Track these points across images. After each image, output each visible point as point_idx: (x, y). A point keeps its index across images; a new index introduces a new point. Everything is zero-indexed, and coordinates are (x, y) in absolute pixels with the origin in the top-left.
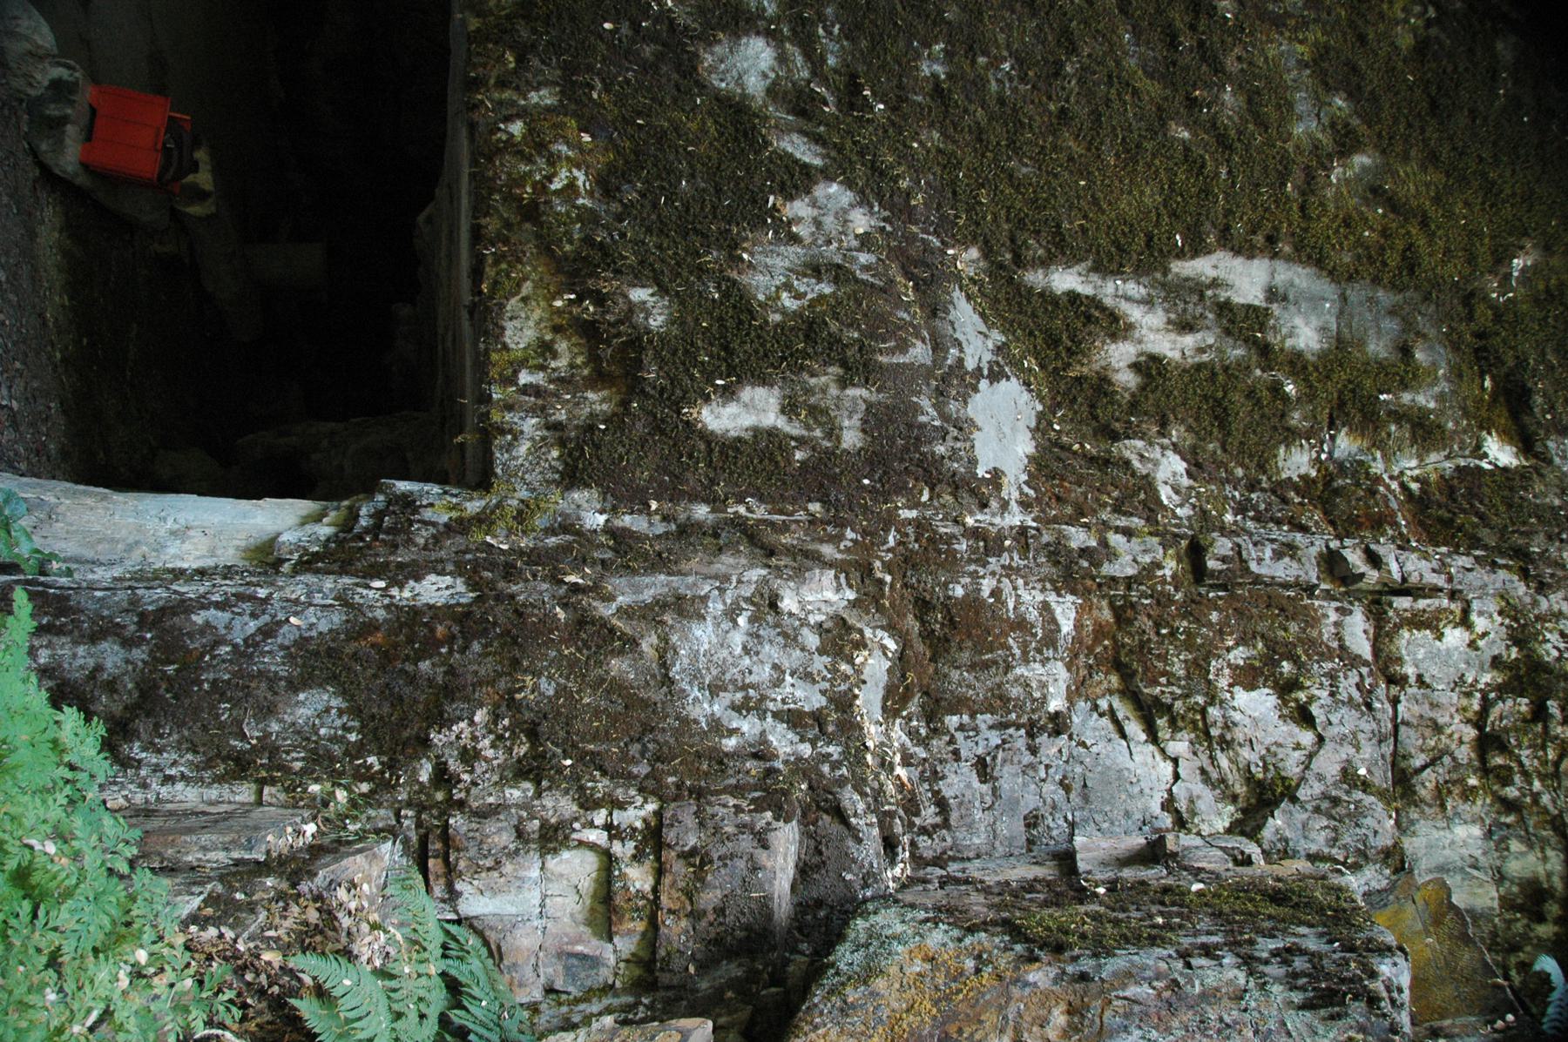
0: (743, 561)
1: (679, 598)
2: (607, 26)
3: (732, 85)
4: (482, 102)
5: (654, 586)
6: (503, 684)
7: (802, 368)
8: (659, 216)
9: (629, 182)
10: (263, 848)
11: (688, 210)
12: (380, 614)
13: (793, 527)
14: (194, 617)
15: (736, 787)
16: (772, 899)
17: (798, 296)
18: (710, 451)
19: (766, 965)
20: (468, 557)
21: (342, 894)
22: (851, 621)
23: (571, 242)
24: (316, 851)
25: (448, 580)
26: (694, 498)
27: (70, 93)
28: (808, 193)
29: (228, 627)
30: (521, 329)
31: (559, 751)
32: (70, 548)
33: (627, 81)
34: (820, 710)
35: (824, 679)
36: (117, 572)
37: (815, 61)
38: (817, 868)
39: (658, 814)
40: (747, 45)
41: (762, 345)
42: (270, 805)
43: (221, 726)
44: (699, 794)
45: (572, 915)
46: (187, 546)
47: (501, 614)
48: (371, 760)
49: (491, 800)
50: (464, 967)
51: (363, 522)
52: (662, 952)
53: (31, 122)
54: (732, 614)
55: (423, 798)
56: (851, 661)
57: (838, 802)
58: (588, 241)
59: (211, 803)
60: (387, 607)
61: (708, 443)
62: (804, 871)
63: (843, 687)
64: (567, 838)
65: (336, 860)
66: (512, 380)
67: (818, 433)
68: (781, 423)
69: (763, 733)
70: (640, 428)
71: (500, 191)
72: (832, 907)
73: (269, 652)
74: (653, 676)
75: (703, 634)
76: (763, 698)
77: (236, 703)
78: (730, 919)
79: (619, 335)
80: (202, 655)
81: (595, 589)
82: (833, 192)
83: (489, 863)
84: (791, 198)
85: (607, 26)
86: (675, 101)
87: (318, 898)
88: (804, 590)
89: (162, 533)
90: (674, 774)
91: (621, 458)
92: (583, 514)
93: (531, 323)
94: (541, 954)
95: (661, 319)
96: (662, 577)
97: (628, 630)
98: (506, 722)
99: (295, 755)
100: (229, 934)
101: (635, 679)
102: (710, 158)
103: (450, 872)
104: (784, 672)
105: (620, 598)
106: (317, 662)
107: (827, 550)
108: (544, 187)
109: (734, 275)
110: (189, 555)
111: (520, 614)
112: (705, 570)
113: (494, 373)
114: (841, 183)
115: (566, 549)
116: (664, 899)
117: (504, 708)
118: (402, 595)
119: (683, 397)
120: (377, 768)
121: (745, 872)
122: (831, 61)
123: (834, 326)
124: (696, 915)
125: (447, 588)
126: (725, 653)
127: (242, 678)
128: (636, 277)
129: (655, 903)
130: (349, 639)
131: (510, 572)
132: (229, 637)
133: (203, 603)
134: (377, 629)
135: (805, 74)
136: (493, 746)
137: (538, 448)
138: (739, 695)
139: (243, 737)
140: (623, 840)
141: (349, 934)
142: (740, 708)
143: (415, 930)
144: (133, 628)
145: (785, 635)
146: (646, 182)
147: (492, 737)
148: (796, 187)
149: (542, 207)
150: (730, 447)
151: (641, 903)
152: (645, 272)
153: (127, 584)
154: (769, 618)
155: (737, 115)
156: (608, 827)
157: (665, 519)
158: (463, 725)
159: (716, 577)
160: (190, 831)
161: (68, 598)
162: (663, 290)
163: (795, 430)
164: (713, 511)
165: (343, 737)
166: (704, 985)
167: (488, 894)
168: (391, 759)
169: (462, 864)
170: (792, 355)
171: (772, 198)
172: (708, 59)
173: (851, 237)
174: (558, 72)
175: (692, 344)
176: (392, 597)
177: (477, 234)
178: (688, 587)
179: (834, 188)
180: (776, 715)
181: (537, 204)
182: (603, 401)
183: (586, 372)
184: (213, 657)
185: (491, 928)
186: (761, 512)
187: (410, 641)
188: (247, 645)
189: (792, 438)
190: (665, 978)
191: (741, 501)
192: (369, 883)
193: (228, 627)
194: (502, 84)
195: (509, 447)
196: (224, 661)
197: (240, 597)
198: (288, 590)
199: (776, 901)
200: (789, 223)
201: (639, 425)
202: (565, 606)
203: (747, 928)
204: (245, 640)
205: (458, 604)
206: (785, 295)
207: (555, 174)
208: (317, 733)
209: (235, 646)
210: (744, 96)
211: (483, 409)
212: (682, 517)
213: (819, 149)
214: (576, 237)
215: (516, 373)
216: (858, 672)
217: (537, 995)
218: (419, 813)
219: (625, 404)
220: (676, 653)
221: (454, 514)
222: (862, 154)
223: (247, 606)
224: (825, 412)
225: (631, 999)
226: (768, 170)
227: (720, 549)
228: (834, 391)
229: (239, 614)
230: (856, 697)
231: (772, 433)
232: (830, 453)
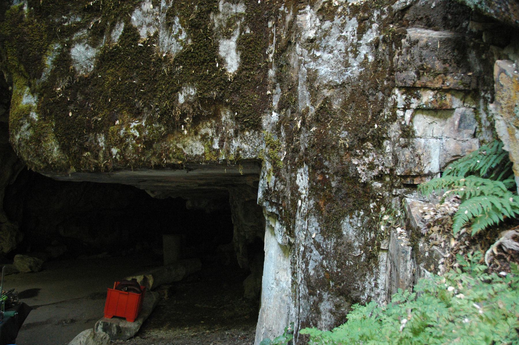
0: (293, 54)
1: (308, 80)
2: (70, 114)
3: (92, 63)
4: (104, 165)
5: (303, 91)
6: (342, 153)
7: (211, 30)
8: (149, 92)
9: (135, 104)
10: (407, 247)
11: (146, 80)
12: (312, 202)
13: (278, 33)
14: (311, 274)
15: (390, 55)
16: (441, 38)
17: (180, 32)
18: (246, 69)
19: (472, 41)
20: (289, 167)
21: (427, 217)
22: (320, 7)
23: (160, 128)
24: (408, 227)
25: (298, 175)
26: (266, 76)
28: (136, 29)
29: (316, 261)
30: (196, 148)
31: (371, 129)
32: (283, 323)
33: (93, 106)
34: (358, 20)
35: (344, 19)
36: (292, 306)
37: (79, 27)
38: (428, 19)
39: (400, 88)
40: (74, 56)
41: (201, 47)
42: (388, 246)
43: (356, 264)
44: (392, 71)
45: (442, 126)
46: (283, 279)
47: (312, 153)
48: (371, 206)
49: (390, 158)
50: (461, 170)
51: (274, 210)
52: (461, 87)
54: (315, 58)
55: (388, 185)
56: (337, 7)
57: (399, 10)
58: (160, 121)
59: (387, 269)
60: (309, 199)
61: (243, 70)
62: (429, 25)
63: (348, 10)
64: (408, 127)
65: (413, 219)
66: (217, 151)
67: (238, 23)
68: (234, 39)
69: (367, 44)
70: (237, 98)
71: (141, 157)
72: (447, 12)
73: (326, 245)
74: (341, 91)
75: (323, 70)
76: (352, 44)
77: (347, 259)
78: (449, 57)
79: (198, 107)
80: (327, 271)
81: (303, 115)
82: (136, 18)
83: (417, 159)
84: (139, 36)
85: (70, 114)
86: (100, 86)
87: (429, 226)
88: (305, 28)
89: (277, 289)
90: (383, 82)
91: (249, 106)
92: (272, 121)
93: (194, 144)
94: (458, 139)
95: (191, 90)
96: (299, 88)
97: (321, 101)
98: (358, 151)
100: (442, 260)
101: (342, 98)
102: (123, 71)
103: (421, 175)
104: (341, 36)
105: (308, 105)
106: (331, 226)
107: (288, 18)
109: (172, 60)
110: (286, 278)
111: (313, 146)
112: (297, 70)
113: (214, 159)
114: (131, 15)
115: (286, 128)
116: (438, 86)
117: (352, 152)
118: (304, 193)
119: (224, 80)
120: (375, 204)
121: (428, 50)
122: (79, 20)
123: (193, 16)
124: (446, 72)
125: (302, 176)
126: (332, 61)
127: (336, 256)
128: (174, 100)
129: (439, 90)
130: (322, 214)
131: (296, 150)
132: (320, 261)
133: (306, 271)
134: (318, 203)
135: (85, 31)
136: (368, 157)
137: (245, 140)
138: (350, 55)
139: (360, 256)
140: (410, 103)
141: (444, 215)
142: (356, 55)
143: (445, 186)
144: (315, 298)
145: (325, 36)
146: (134, 97)
147: (364, 157)
148: (134, 34)
149: (147, 140)
150: (244, 60)
151: (438, 96)
152: (172, 97)
153: (297, 301)
154: (317, 42)
155: (104, 60)
156: (404, 110)
157: (274, 88)
158: (358, 169)
159: (299, 66)
160: (398, 276)
161: (303, 322)
162: (179, 89)
163: (237, 33)
164: (271, 68)
165: (362, 217)
166: (478, 68)
167: (430, 160)
168: (372, 198)
169: (417, 170)
170: (206, 35)
171: (139, 45)
172: (82, 73)
173: (154, 10)
174: (91, 134)
175: (202, 77)
176: (305, 198)
177: (158, 167)
178: (303, 77)
179: (134, 18)
180: (359, 39)
181: (145, 142)
182: (225, 114)
183: (214, 121)
184: (328, 267)
185: (445, 159)
186: (272, 48)
187: (323, 190)
188: (323, 254)
189: (241, 34)
190: (473, 85)
191: (267, 56)
192: (423, 207)
193: (316, 261)
194: (97, 157)
195: (245, 152)
196: (329, 263)
197: (304, 257)
198: (301, 239)
199: (442, 36)
200: (149, 37)
201: (236, 99)
202: (310, 127)
203: (453, 50)
204: (321, 255)
205: (308, 171)
206: (180, 38)
207: (133, 135)
208: (360, 227)
209: (323, 259)
210: (96, 57)
211: (229, 163)
212: (274, 81)
213: (117, 25)
214: (158, 126)
215: (214, 150)
216: (342, 4)
217: (476, 141)
218: (395, 187)
219: (227, 105)
220: (331, 81)
221: (272, 174)
222: (118, 6)
223: (307, 254)
224: (229, 20)
225: (482, 101)
226: (127, 46)
227: (288, 64)
228: (220, 16)
229: (310, 257)
230: (353, 5)
231: (238, 43)
232: (247, 18)
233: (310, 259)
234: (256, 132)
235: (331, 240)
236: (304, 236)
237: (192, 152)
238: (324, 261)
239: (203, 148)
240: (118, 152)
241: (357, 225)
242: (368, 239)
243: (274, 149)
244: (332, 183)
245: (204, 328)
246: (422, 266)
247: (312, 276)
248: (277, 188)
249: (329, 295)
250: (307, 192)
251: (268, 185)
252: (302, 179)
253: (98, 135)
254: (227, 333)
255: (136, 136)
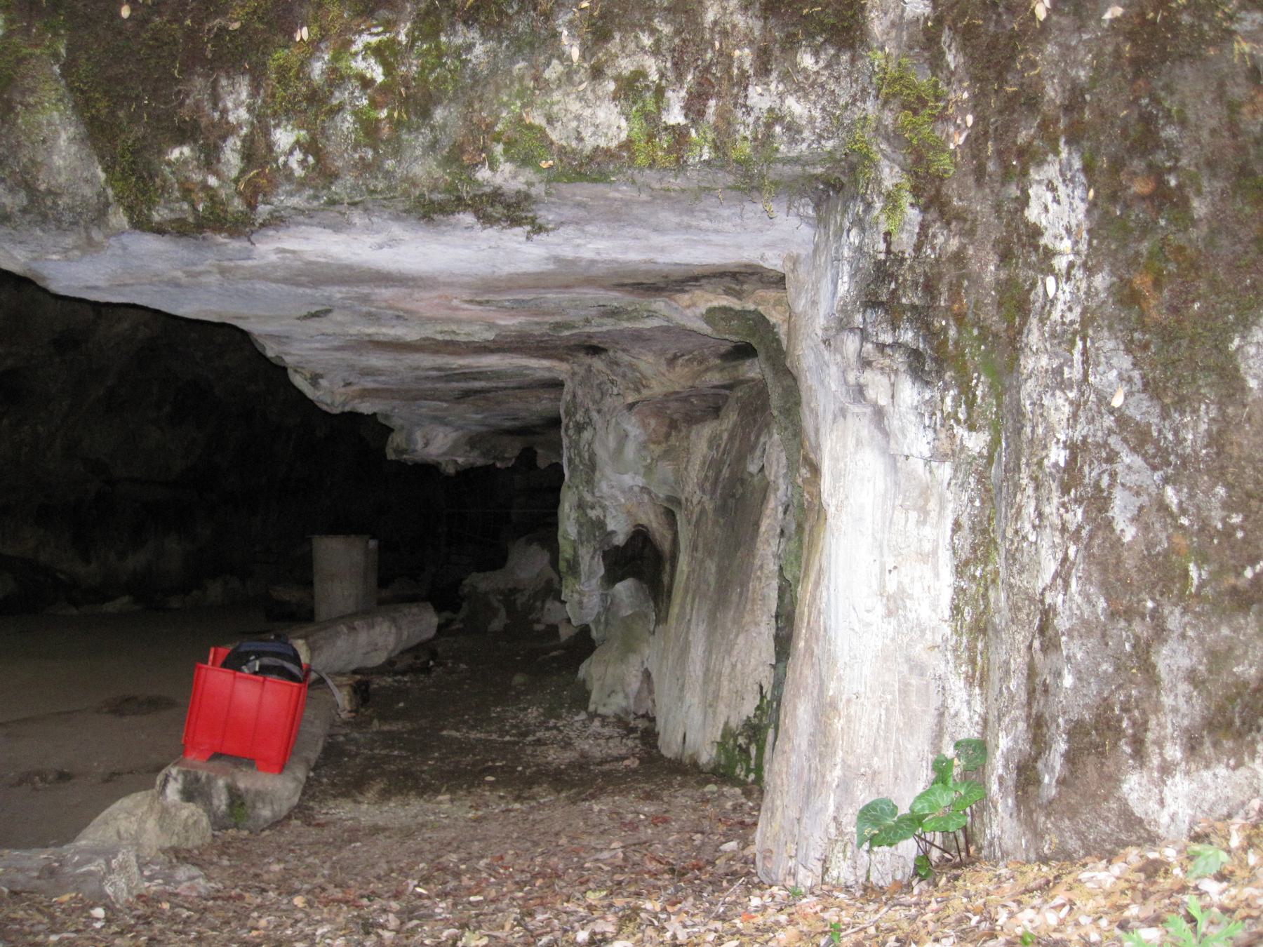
12: (1101, 281)
14: (1127, 538)
23: (469, 47)
27: (197, 780)
36: (957, 685)
46: (916, 590)
51: (907, 336)
53: (236, 826)
60: (1090, 271)
66: (679, 134)
73: (1176, 434)
89: (890, 627)
92: (909, 14)
93: (587, 112)
108: (385, 89)
115: (968, 36)
144: (1137, 627)
176: (1071, 265)
184: (1184, 512)
195: (793, 130)
196: (1192, 496)
204: (1155, 468)
221: (907, 199)
229: (1113, 475)
233: (1111, 486)
234: (845, 57)
235: (1195, 411)
236: (1067, 409)
237: (580, 139)
238: (1169, 491)
239: (623, 124)
240: (297, 142)
243: (915, 112)
244: (1195, 203)
245: (501, 798)
247: (1130, 547)
248: (933, 248)
249: (1186, 619)
250: (1083, 247)
251: (889, 244)
252: (1057, 201)
253: (224, 82)
254: (596, 808)
255: (372, 81)
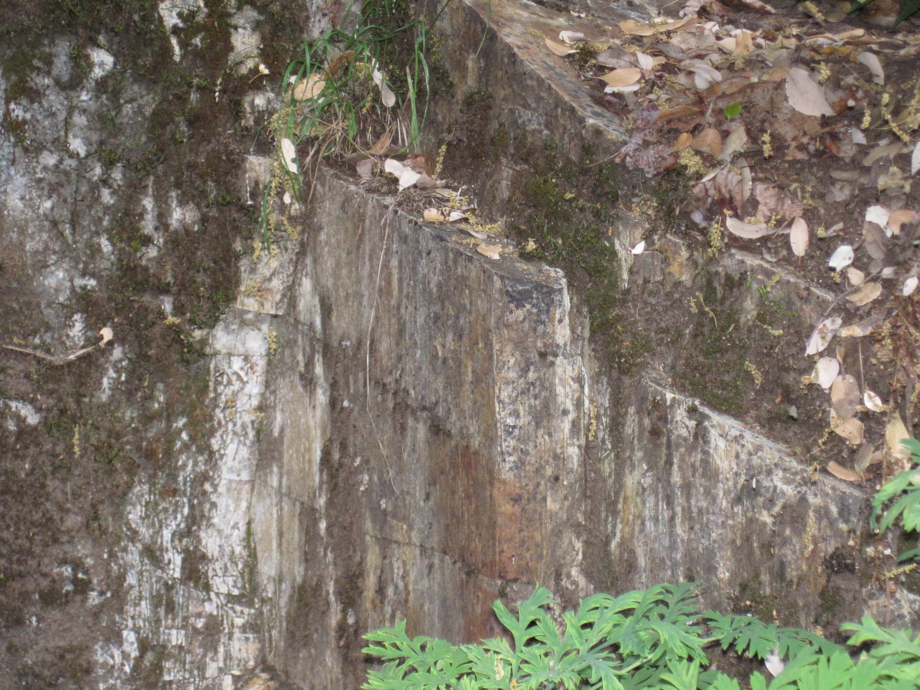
99: (148, 225)
139: (89, 365)
165: (101, 85)
241: (61, 146)
242: (147, 241)
246: (658, 380)
